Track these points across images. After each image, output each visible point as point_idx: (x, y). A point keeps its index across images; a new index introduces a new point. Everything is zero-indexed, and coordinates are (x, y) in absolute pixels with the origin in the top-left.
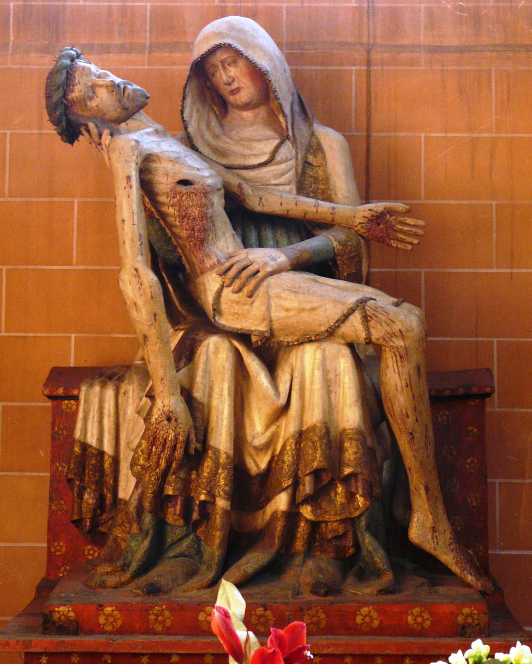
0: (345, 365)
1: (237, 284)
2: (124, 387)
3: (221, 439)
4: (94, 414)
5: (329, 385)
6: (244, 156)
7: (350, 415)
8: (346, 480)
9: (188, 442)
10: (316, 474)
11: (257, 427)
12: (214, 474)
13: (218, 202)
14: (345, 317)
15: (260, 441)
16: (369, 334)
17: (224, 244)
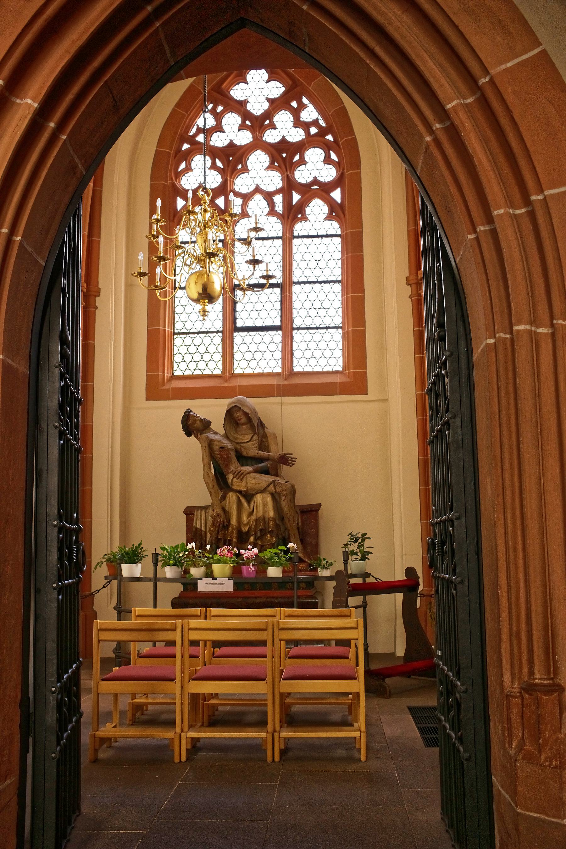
0: (269, 499)
1: (238, 477)
2: (208, 511)
3: (234, 522)
4: (199, 518)
5: (265, 505)
6: (242, 439)
7: (271, 514)
8: (271, 532)
9: (224, 522)
10: (261, 530)
11: (245, 518)
12: (232, 531)
13: (233, 454)
14: (269, 486)
15: (245, 522)
16: (276, 490)
17: (235, 466)
